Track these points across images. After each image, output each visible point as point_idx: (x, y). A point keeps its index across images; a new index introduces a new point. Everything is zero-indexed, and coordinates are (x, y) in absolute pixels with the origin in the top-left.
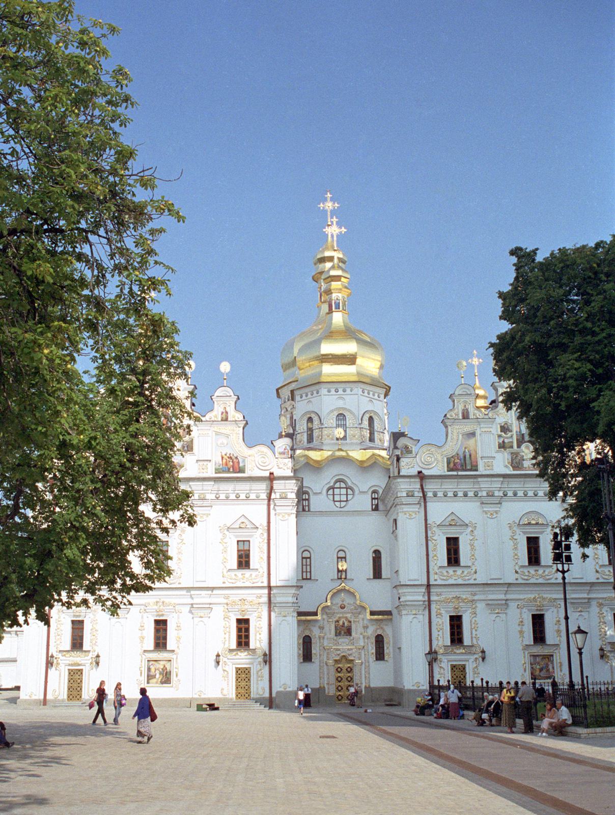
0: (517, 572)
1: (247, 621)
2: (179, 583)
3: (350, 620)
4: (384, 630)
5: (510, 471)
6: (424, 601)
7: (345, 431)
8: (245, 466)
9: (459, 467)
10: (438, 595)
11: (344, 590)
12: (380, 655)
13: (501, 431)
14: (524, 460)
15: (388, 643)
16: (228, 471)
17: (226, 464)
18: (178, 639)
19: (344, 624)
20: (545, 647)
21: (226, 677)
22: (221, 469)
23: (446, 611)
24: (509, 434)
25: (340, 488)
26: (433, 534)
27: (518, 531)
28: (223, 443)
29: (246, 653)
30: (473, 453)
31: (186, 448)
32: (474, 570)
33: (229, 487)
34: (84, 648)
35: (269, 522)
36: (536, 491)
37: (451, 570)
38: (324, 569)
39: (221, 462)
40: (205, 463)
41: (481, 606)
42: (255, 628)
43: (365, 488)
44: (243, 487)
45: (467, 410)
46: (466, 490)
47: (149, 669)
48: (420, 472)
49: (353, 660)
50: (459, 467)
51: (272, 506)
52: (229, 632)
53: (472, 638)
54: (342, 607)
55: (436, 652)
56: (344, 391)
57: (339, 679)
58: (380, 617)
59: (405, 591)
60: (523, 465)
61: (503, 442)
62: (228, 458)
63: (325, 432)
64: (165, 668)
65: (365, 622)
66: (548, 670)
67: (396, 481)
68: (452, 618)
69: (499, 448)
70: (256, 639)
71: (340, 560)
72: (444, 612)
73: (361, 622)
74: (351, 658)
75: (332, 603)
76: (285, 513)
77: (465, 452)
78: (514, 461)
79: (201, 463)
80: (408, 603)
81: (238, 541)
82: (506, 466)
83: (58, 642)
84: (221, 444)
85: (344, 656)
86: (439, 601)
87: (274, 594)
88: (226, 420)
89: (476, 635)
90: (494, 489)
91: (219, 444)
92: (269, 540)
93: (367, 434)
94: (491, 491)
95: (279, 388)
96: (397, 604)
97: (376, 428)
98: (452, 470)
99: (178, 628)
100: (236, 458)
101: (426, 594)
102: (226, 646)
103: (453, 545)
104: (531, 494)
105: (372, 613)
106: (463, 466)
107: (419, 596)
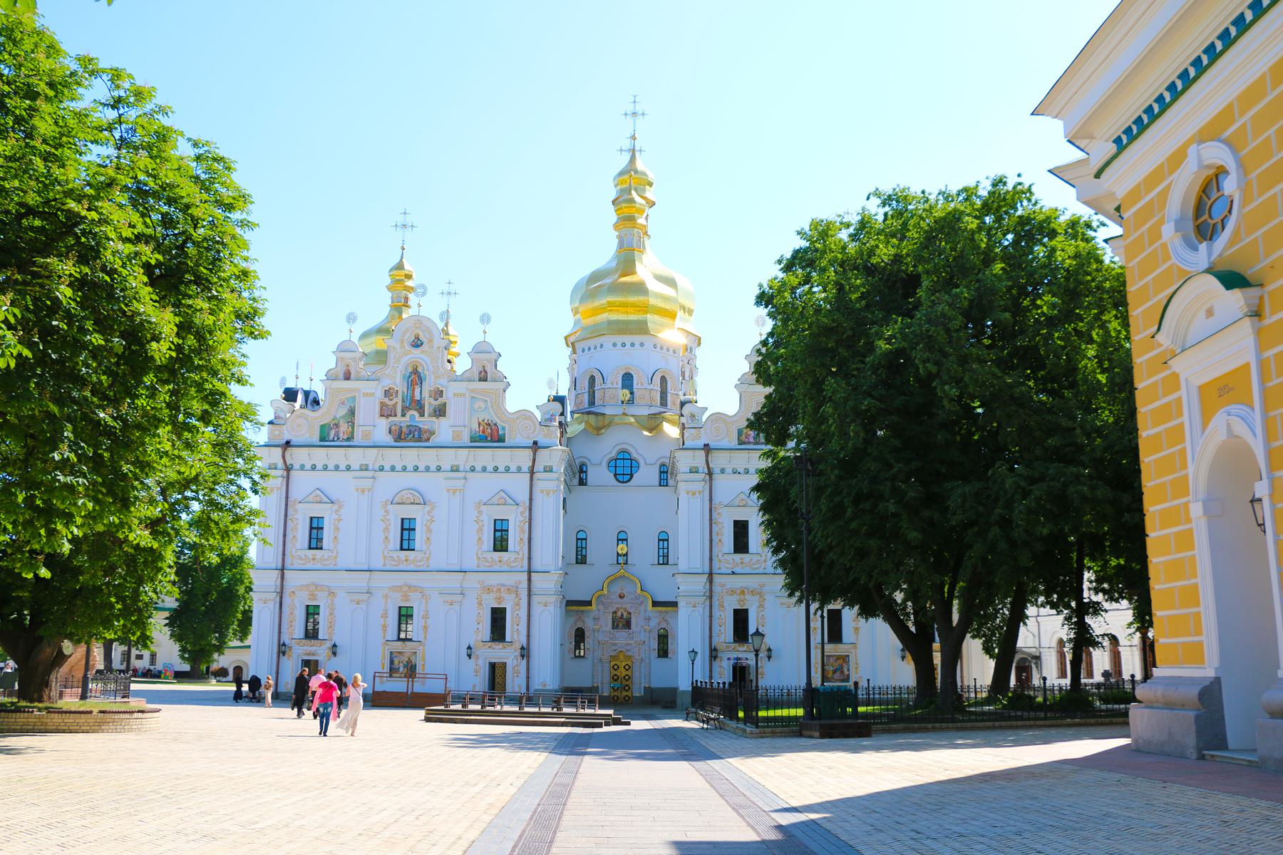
1: (503, 611)
7: (632, 393)
9: (752, 440)
11: (623, 577)
12: (663, 652)
16: (486, 440)
17: (484, 432)
19: (622, 615)
20: (840, 646)
21: (476, 671)
25: (624, 459)
29: (501, 645)
33: (486, 457)
34: (320, 636)
35: (531, 500)
37: (738, 557)
38: (602, 552)
40: (459, 429)
41: (769, 599)
42: (512, 619)
47: (392, 662)
48: (706, 445)
49: (629, 658)
54: (621, 597)
55: (715, 650)
56: (633, 345)
57: (616, 677)
58: (664, 609)
64: (409, 661)
66: (842, 672)
68: (736, 612)
70: (512, 631)
71: (620, 542)
74: (629, 654)
75: (609, 592)
79: (455, 429)
81: (495, 520)
85: (621, 652)
92: (530, 519)
95: (568, 336)
97: (669, 388)
98: (744, 443)
99: (426, 617)
100: (495, 425)
101: (708, 584)
102: (479, 638)
107: (700, 583)
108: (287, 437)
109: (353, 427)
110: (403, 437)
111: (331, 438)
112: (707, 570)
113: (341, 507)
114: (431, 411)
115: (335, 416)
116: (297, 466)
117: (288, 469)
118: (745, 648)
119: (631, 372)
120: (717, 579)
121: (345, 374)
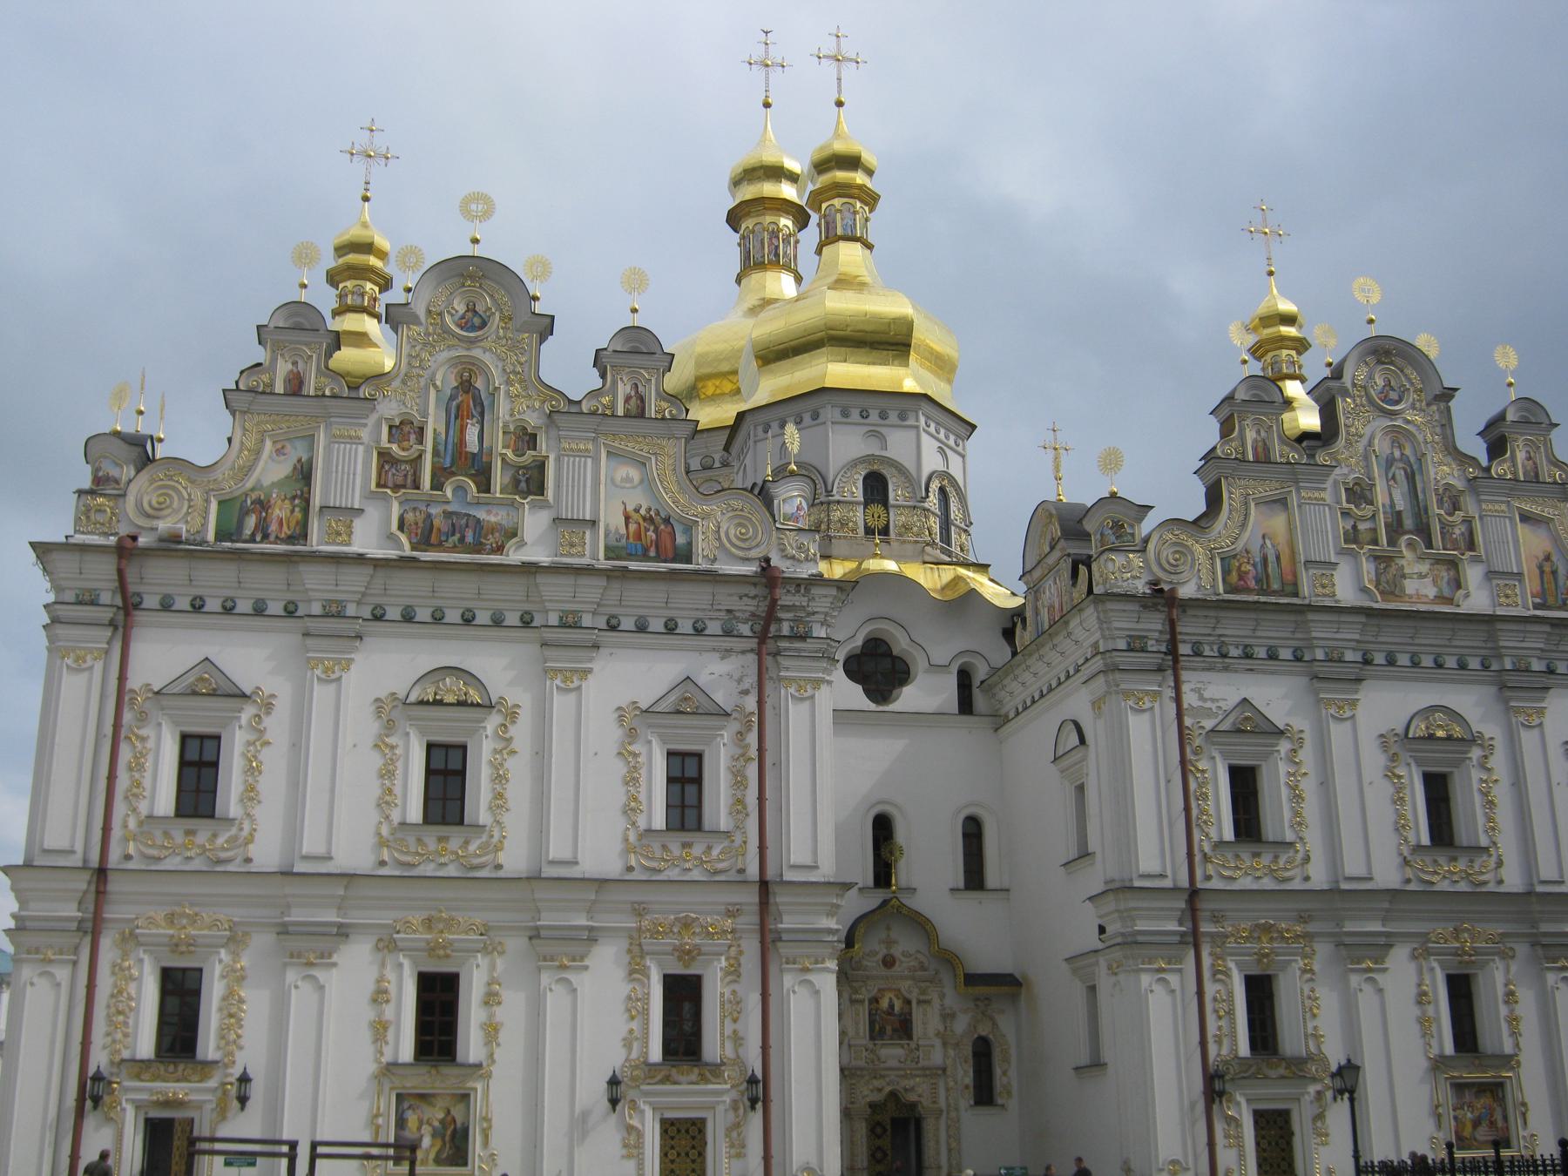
0: (1406, 862)
2: (499, 867)
3: (907, 995)
4: (995, 1024)
6: (1183, 934)
8: (690, 544)
9: (1252, 584)
10: (1216, 918)
13: (1348, 502)
14: (1404, 576)
15: (1006, 1060)
16: (645, 557)
17: (638, 536)
18: (492, 1032)
19: (892, 1006)
22: (623, 548)
23: (1237, 963)
24: (1367, 510)
26: (1195, 753)
27: (1405, 756)
28: (628, 479)
29: (694, 1077)
31: (523, 485)
32: (1300, 856)
36: (1439, 655)
37: (1245, 853)
39: (623, 531)
43: (941, 654)
44: (689, 602)
46: (1272, 642)
50: (1252, 584)
51: (769, 660)
52: (645, 1013)
53: (1306, 1035)
54: (889, 962)
55: (1220, 1076)
56: (883, 415)
59: (1132, 904)
60: (1403, 589)
61: (1354, 527)
62: (644, 519)
63: (836, 515)
65: (948, 1002)
69: (1345, 543)
70: (722, 1034)
72: (1232, 965)
73: (936, 1002)
76: (801, 679)
77: (1262, 546)
78: (1383, 579)
80: (1140, 938)
82: (1364, 590)
83: (119, 1036)
84: (622, 480)
86: (1218, 934)
87: (776, 904)
88: (641, 414)
89: (1315, 1028)
90: (1340, 644)
91: (618, 478)
93: (936, 529)
96: (1094, 941)
100: (667, 521)
101: (1188, 914)
103: (1244, 783)
104: (1427, 661)
105: (972, 979)
106: (1261, 580)
108: (124, 530)
109: (306, 510)
110: (434, 539)
111: (248, 532)
112: (1185, 883)
113: (268, 707)
114: (507, 480)
115: (259, 481)
116: (151, 601)
117: (129, 606)
118: (1281, 1071)
119: (884, 472)
120: (1205, 905)
121: (287, 381)
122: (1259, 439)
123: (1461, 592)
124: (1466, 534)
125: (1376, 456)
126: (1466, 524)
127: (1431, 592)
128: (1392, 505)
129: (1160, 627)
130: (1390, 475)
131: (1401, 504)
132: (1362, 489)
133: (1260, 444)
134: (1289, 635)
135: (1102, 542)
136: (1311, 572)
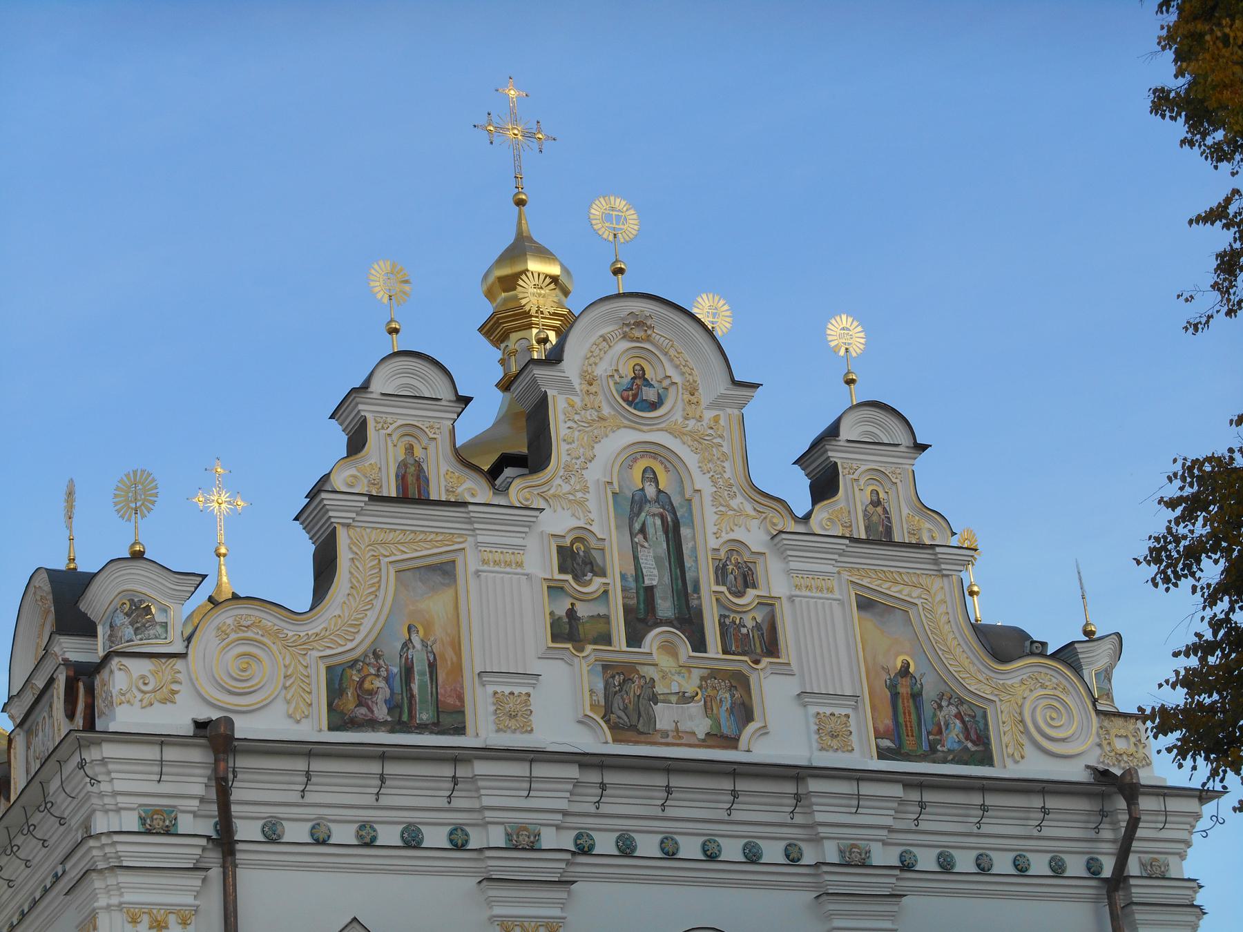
5: (596, 741)
9: (381, 712)
13: (562, 570)
14: (654, 699)
30: (450, 654)
45: (418, 464)
60: (652, 720)
61: (571, 613)
67: (92, 754)
69: (553, 641)
77: (405, 645)
78: (617, 702)
82: (584, 721)
94: (521, 828)
104: (690, 848)
106: (400, 707)
122: (411, 461)
123: (752, 727)
124: (765, 627)
125: (615, 494)
126: (767, 609)
127: (702, 726)
128: (639, 575)
129: (199, 790)
130: (637, 526)
131: (653, 576)
132: (587, 551)
133: (412, 469)
134: (442, 803)
135: (111, 638)
136: (490, 689)
